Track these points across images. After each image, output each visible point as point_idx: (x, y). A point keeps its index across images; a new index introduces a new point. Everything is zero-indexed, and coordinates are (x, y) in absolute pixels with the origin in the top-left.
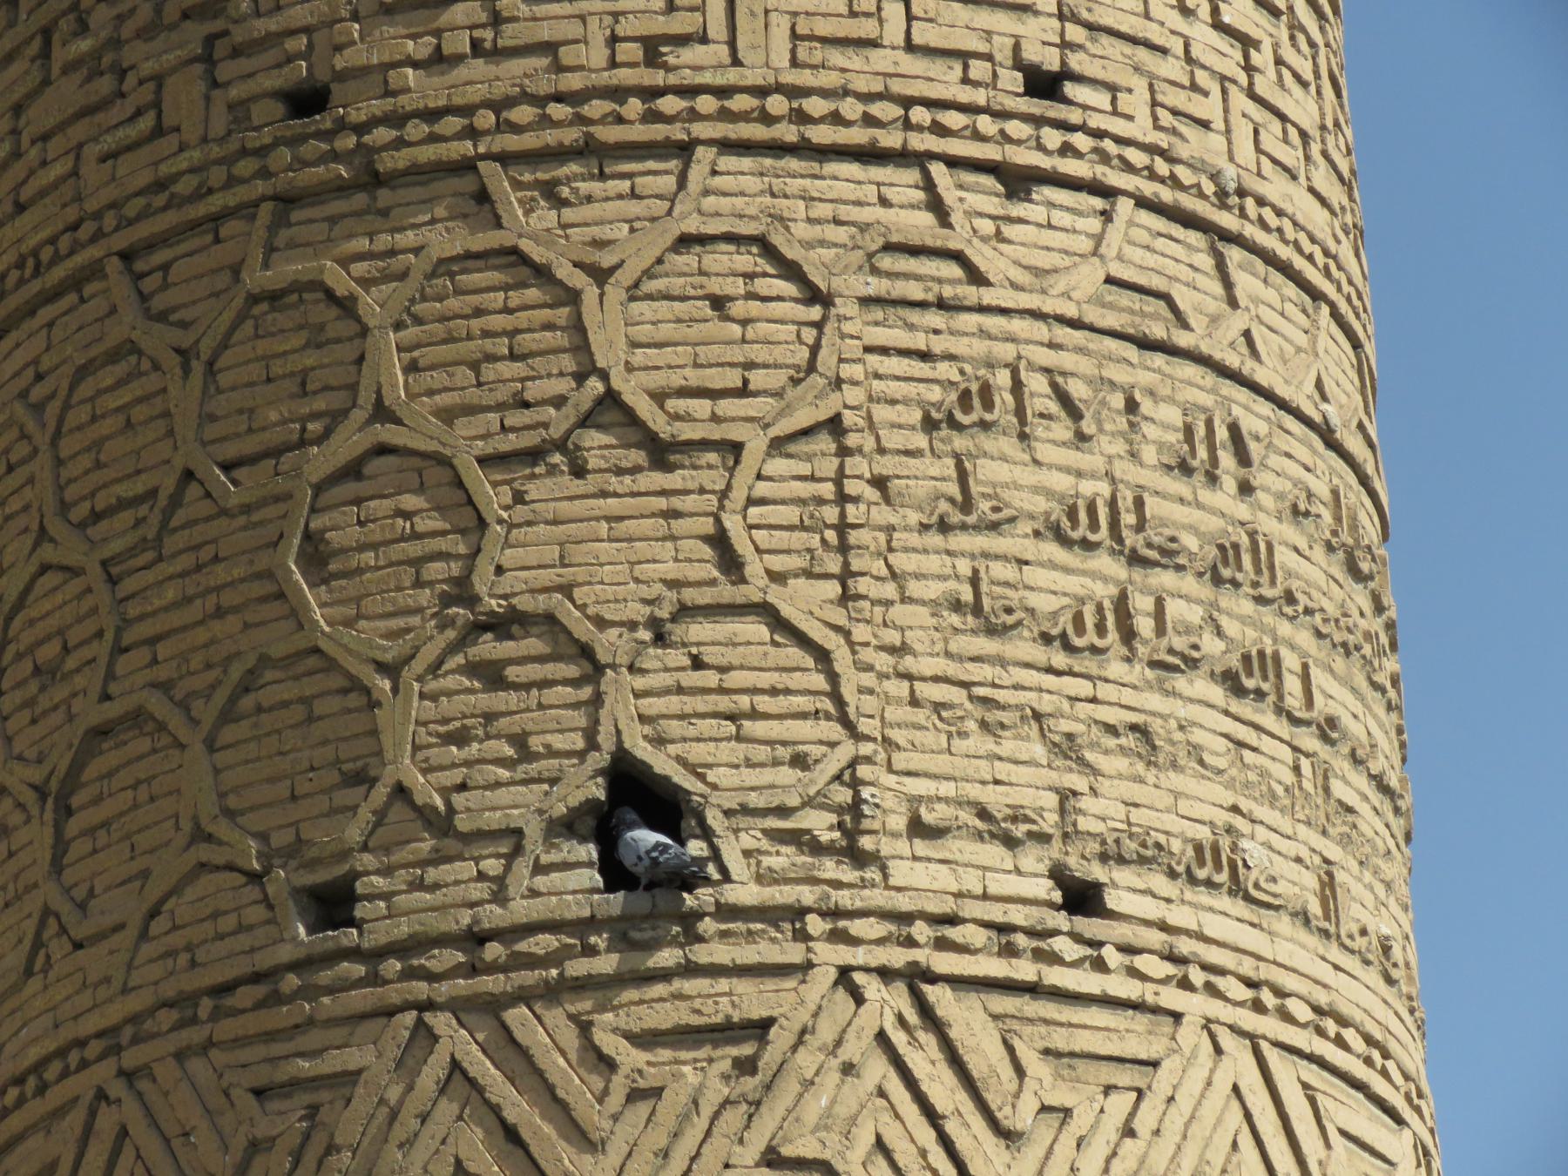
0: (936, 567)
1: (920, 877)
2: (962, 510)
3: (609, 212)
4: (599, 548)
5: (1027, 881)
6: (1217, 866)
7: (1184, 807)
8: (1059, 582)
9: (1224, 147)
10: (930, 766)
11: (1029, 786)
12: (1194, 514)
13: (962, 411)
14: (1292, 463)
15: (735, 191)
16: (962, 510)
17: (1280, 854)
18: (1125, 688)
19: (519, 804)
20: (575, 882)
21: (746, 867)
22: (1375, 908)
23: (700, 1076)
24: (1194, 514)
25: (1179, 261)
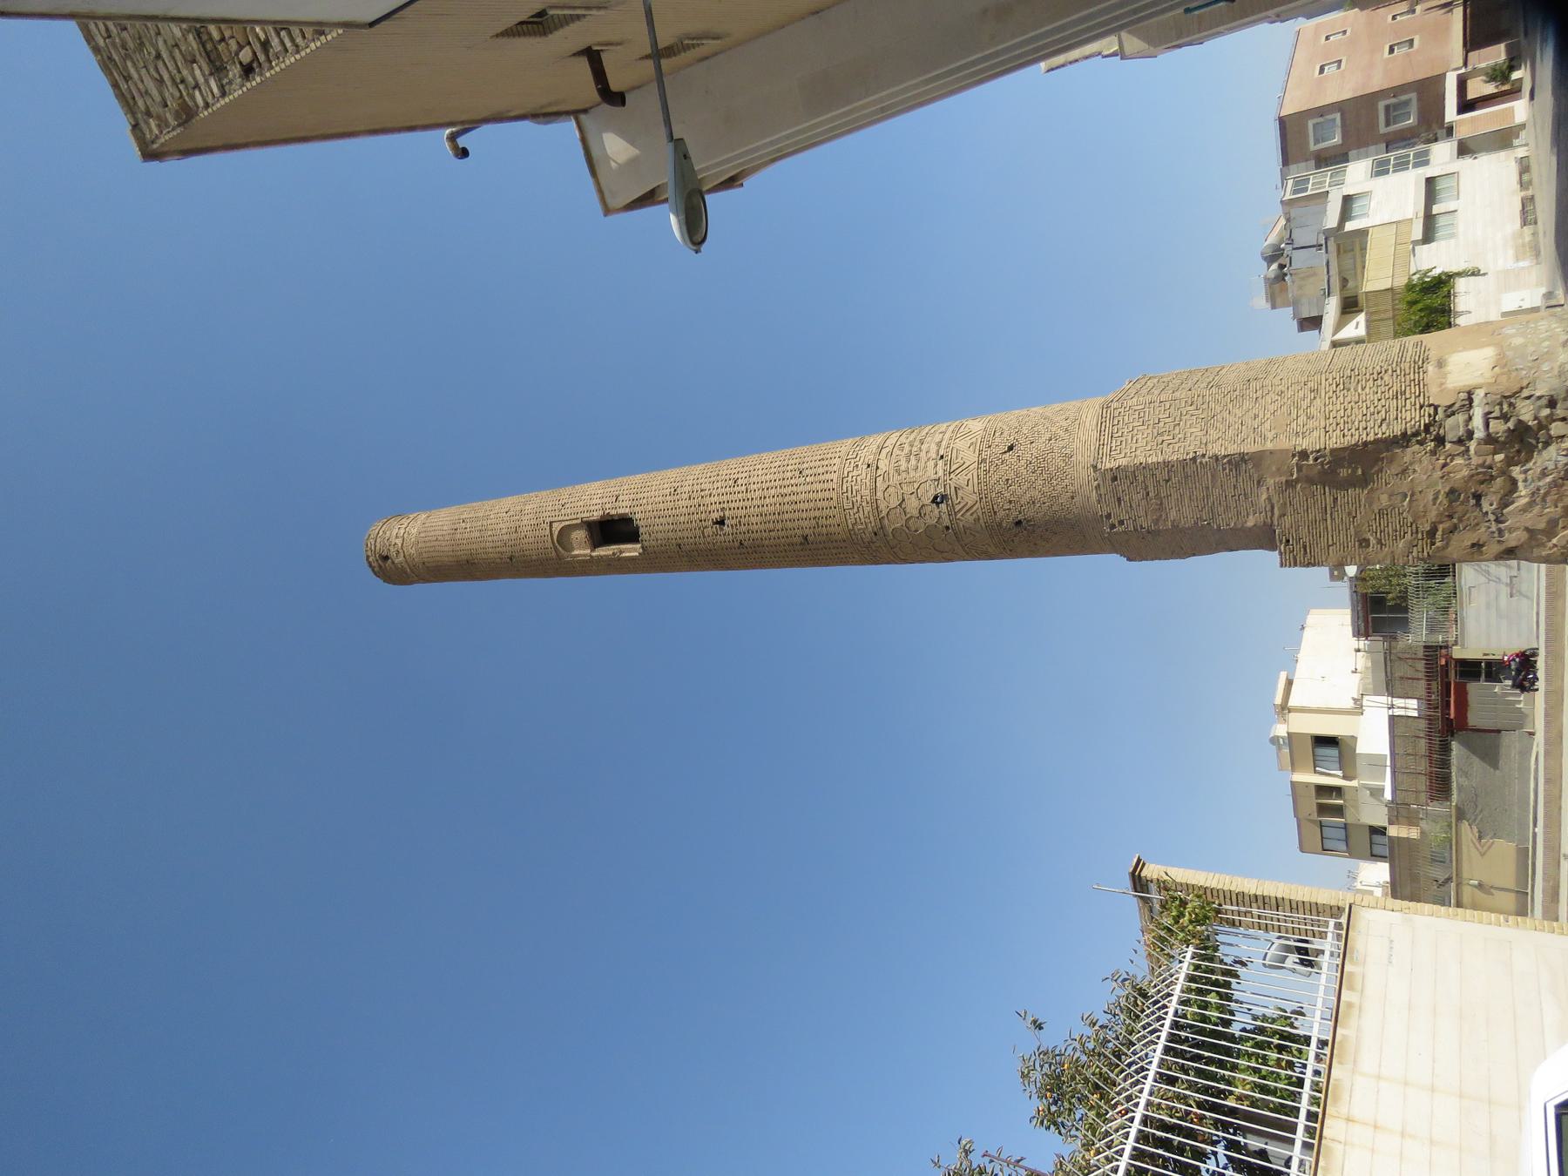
0: (912, 474)
1: (940, 473)
2: (907, 471)
3: (882, 506)
4: (912, 505)
5: (940, 463)
6: (939, 444)
7: (934, 448)
8: (913, 462)
9: (874, 448)
10: (931, 473)
11: (931, 463)
12: (907, 448)
13: (898, 472)
14: (903, 439)
15: (880, 494)
16: (907, 471)
17: (938, 438)
18: (923, 454)
19: (936, 511)
20: (943, 506)
21: (940, 490)
22: (943, 427)
23: (960, 493)
24: (907, 448)
25: (884, 452)
